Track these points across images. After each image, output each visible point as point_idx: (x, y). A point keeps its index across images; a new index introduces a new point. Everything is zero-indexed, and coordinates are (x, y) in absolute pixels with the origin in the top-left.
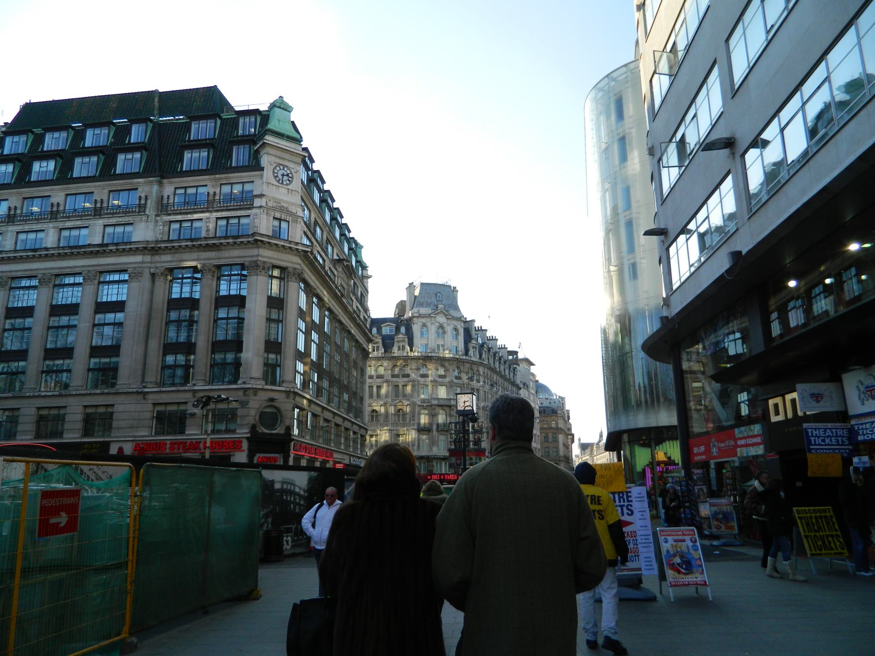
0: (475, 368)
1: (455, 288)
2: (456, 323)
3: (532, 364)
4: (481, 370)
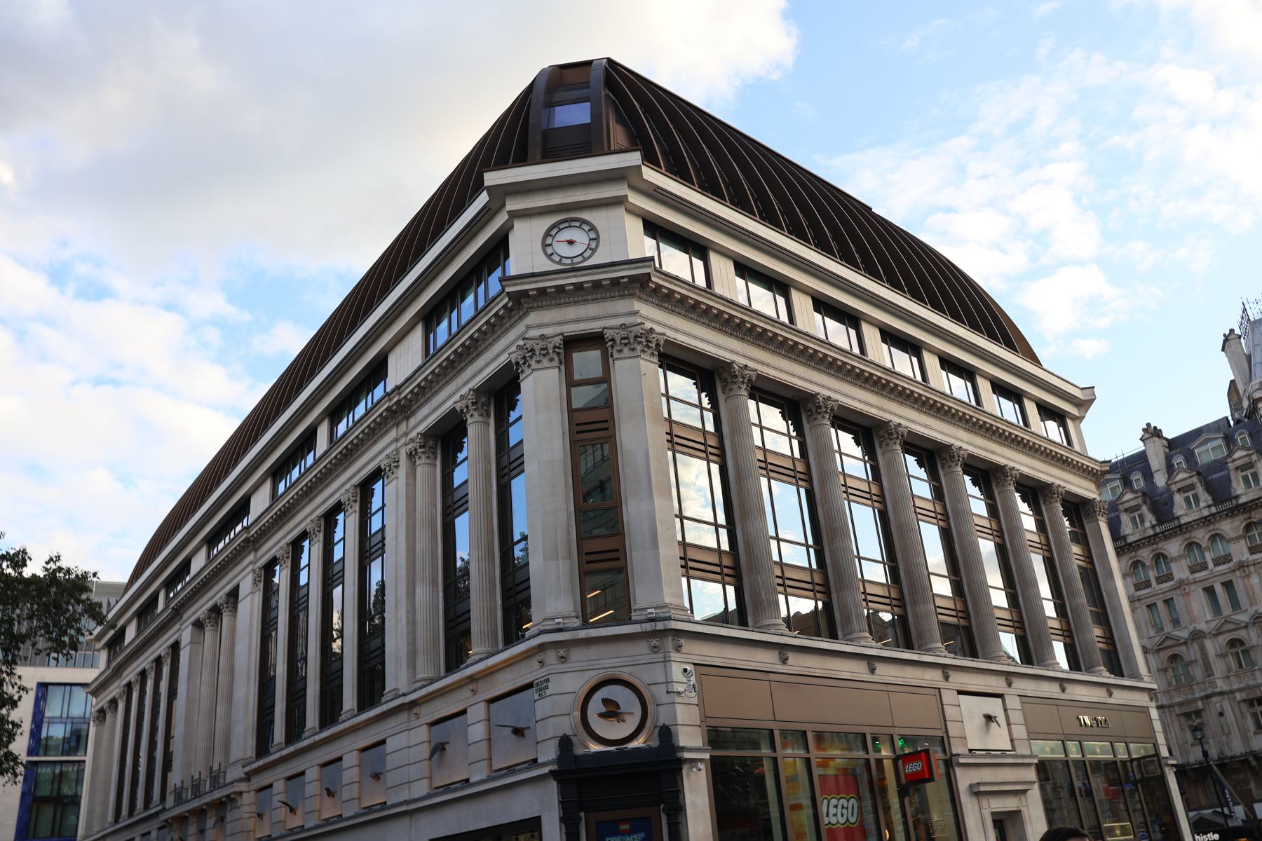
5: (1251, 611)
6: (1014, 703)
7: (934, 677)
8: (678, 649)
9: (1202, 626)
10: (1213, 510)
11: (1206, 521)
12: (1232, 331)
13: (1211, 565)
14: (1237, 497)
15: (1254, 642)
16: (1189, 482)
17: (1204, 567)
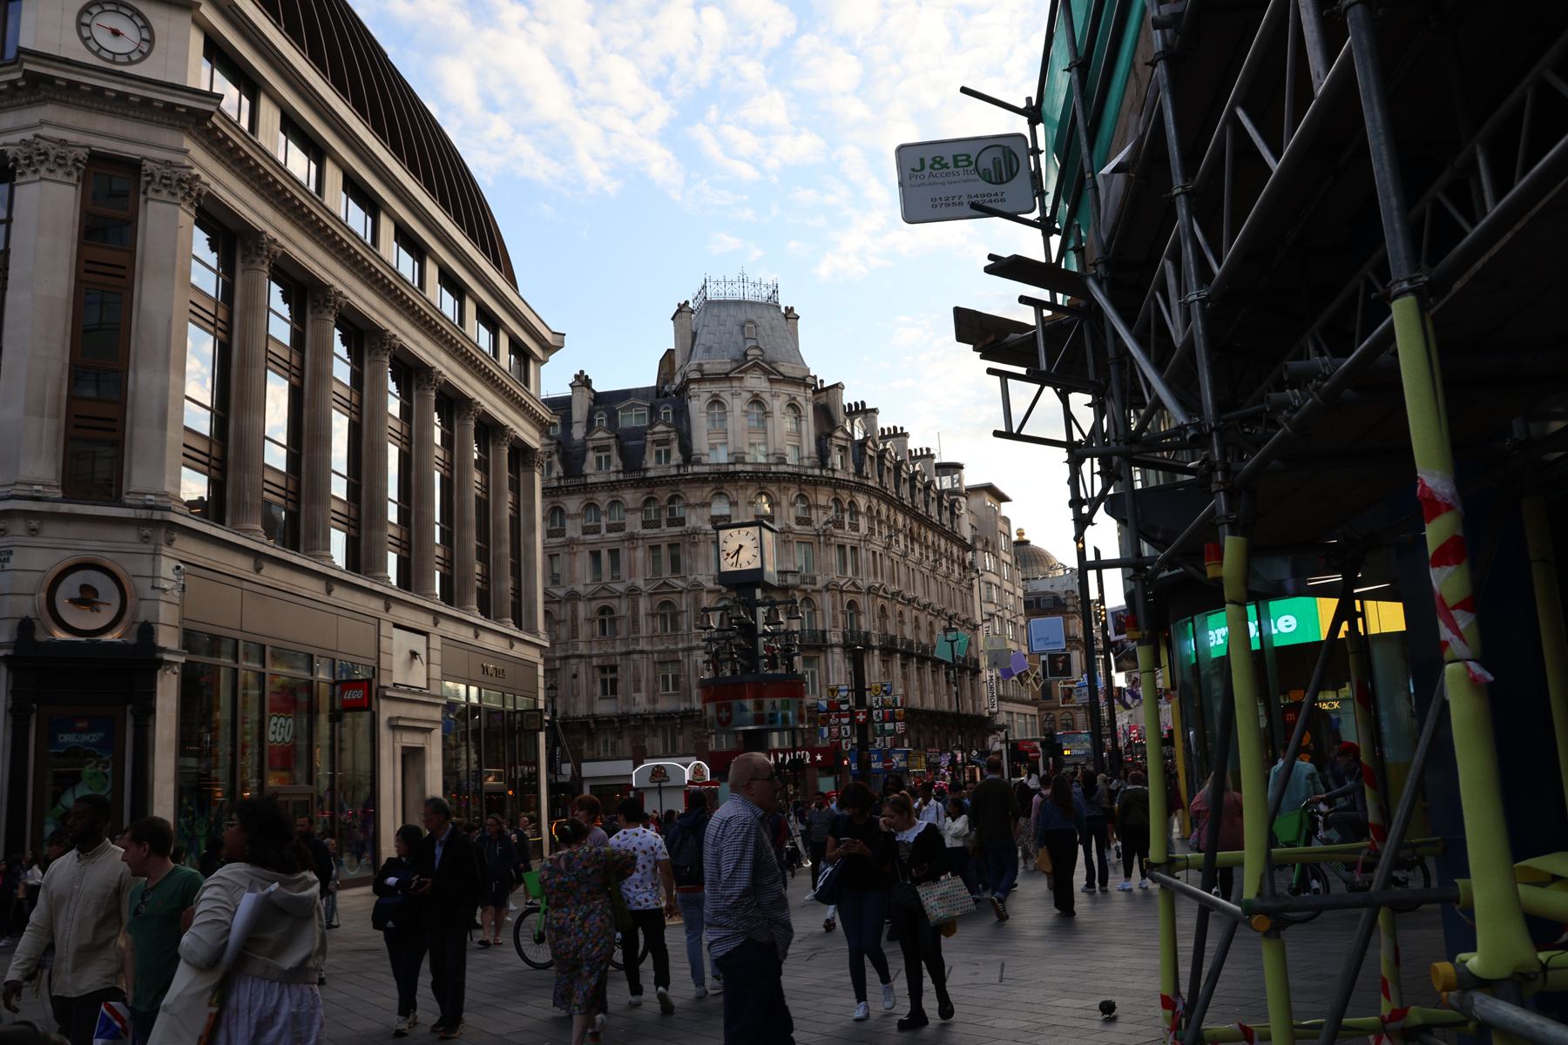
0: (845, 496)
1: (790, 310)
2: (793, 390)
3: (1006, 499)
4: (862, 502)
5: (629, 582)
6: (436, 642)
7: (376, 605)
8: (170, 543)
9: (580, 588)
10: (621, 476)
11: (611, 486)
12: (687, 303)
13: (603, 530)
14: (646, 470)
15: (623, 613)
16: (605, 442)
17: (596, 530)
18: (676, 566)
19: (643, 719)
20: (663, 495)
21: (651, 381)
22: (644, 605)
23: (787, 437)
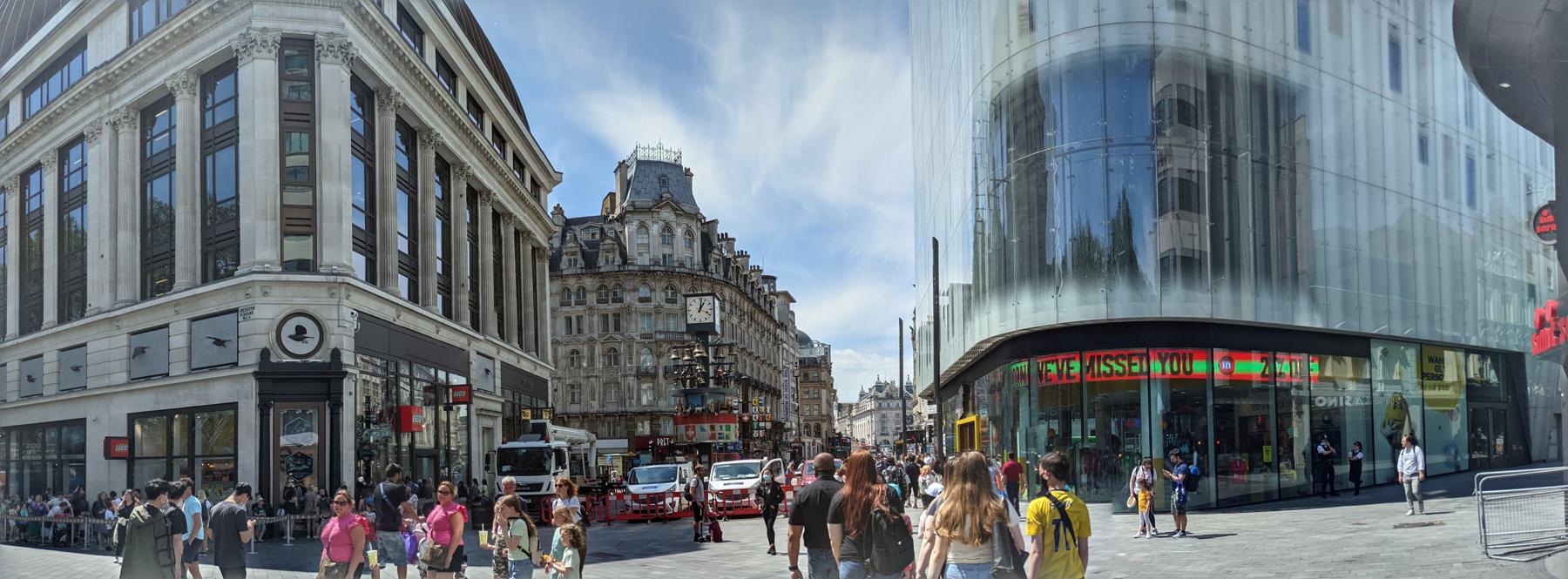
6: (498, 365)
8: (348, 297)
11: (578, 276)
18: (617, 328)
19: (597, 415)
20: (611, 283)
21: (596, 211)
22: (598, 349)
23: (685, 252)
